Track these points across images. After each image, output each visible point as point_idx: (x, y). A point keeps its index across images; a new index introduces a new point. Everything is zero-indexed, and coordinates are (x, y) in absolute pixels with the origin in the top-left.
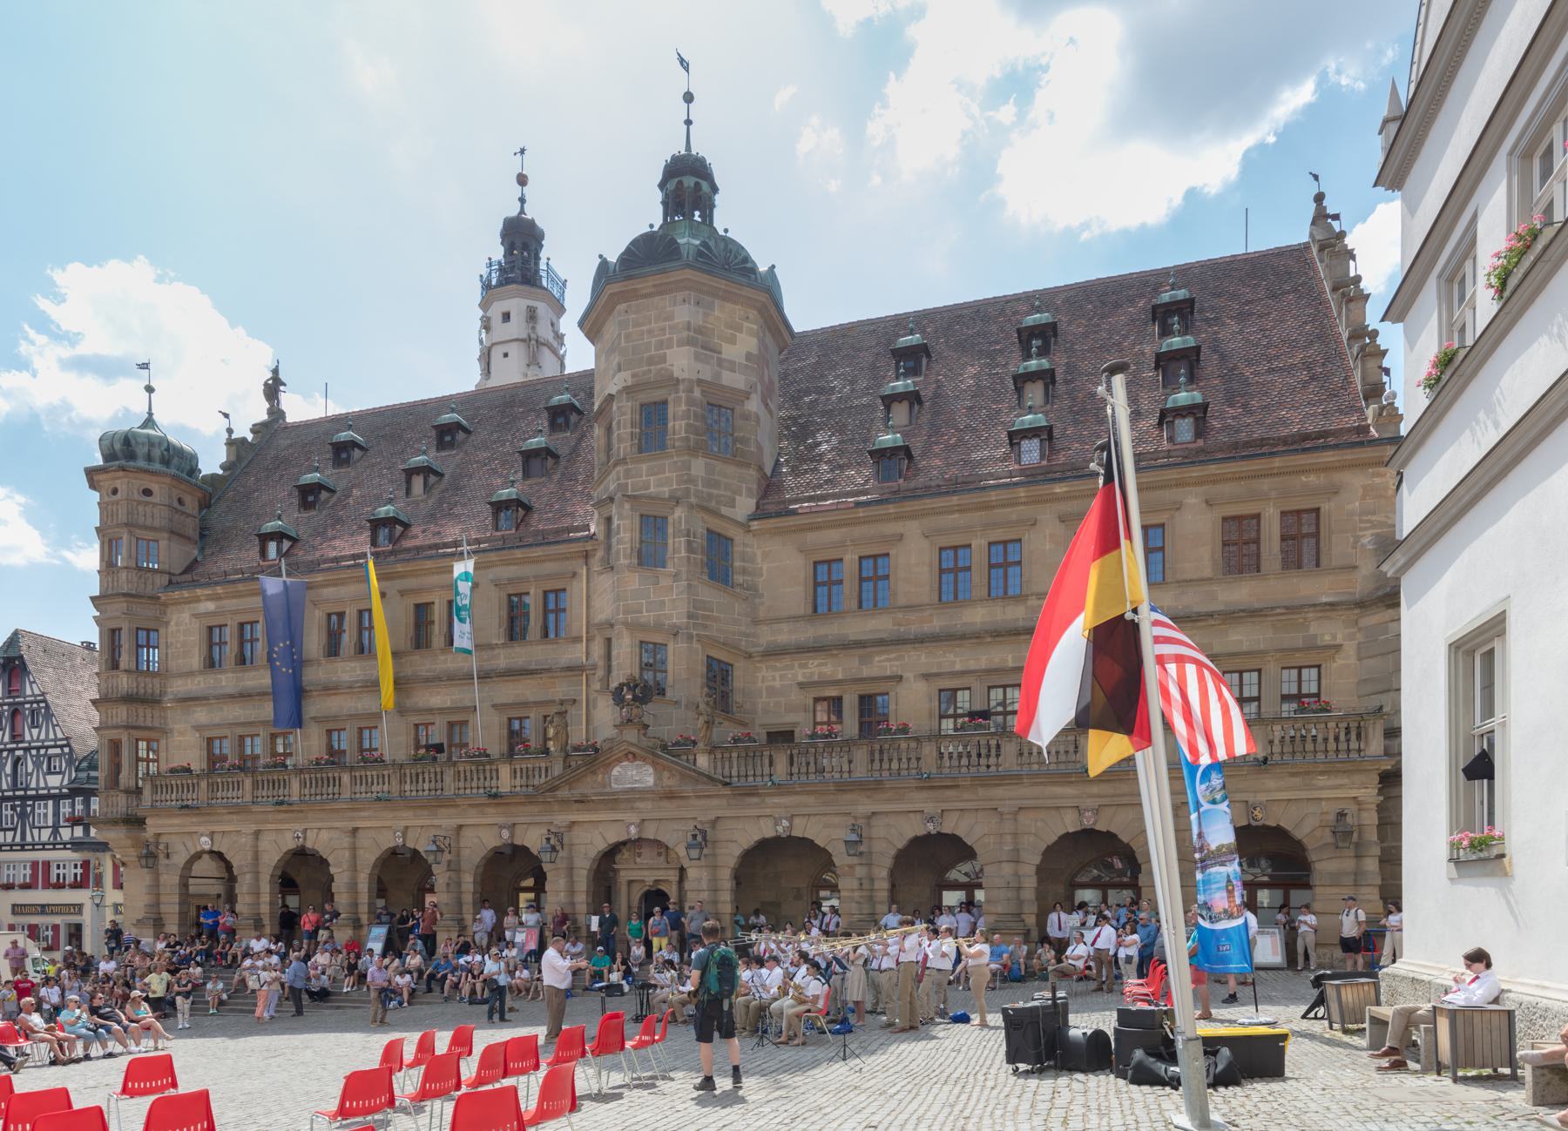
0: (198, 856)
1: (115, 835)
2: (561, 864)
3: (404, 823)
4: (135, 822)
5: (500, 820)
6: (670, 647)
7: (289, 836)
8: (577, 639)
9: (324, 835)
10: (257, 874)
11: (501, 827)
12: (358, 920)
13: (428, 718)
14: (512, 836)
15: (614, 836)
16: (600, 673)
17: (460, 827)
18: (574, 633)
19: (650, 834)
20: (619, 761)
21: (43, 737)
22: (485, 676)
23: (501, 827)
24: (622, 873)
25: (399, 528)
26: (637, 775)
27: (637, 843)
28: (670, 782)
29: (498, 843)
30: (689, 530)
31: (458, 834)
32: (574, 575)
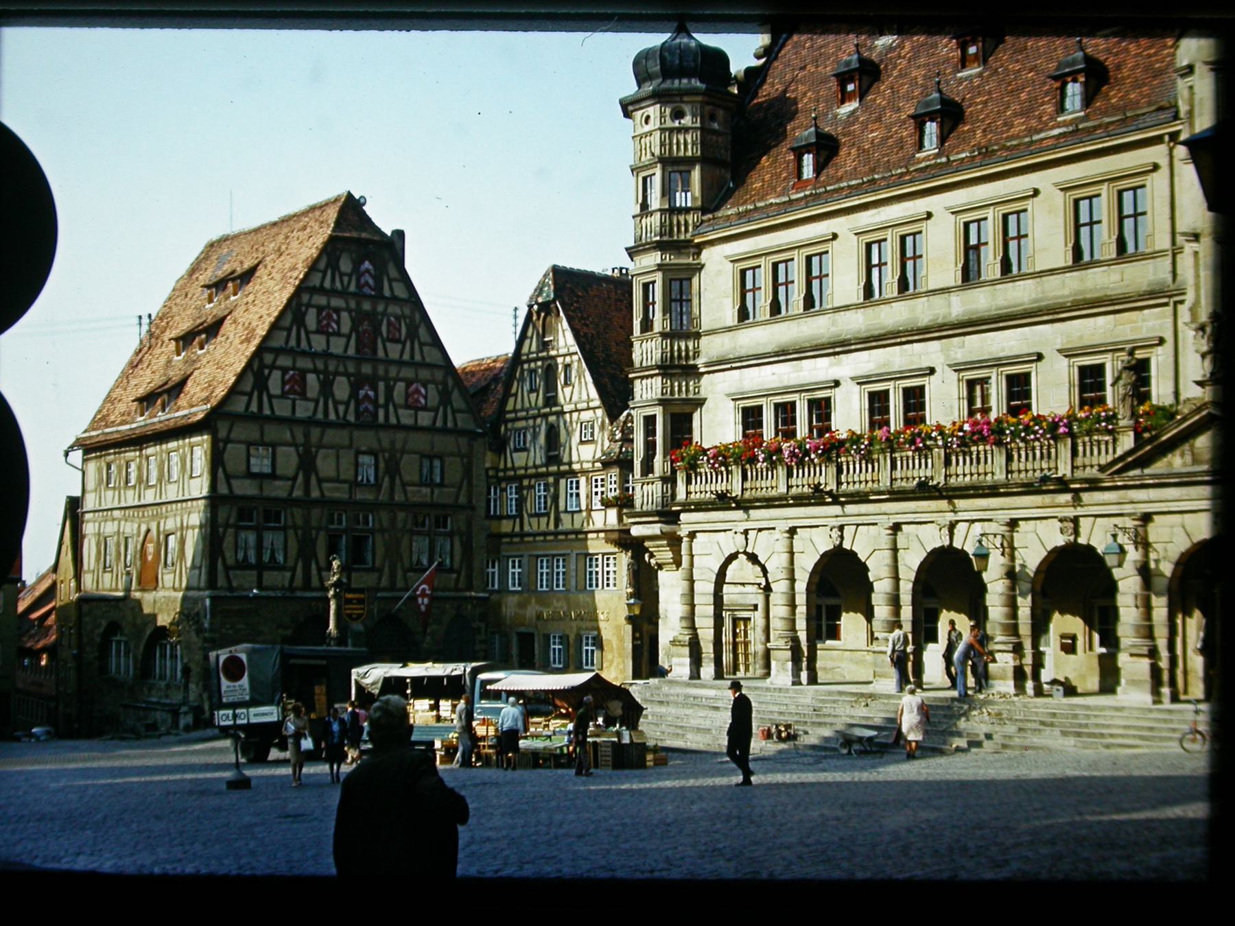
10: (792, 580)
21: (575, 398)
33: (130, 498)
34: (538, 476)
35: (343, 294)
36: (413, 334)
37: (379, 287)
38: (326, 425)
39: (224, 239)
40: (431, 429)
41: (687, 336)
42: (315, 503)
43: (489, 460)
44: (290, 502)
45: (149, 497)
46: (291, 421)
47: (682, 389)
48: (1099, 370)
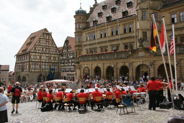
0: (86, 67)
1: (76, 65)
4: (78, 63)
6: (147, 32)
9: (100, 64)
10: (92, 70)
12: (104, 77)
13: (114, 46)
14: (124, 64)
15: (139, 64)
24: (141, 70)
26: (141, 54)
27: (143, 65)
28: (147, 55)
30: (150, 13)
33: (21, 61)
34: (66, 59)
35: (45, 39)
36: (52, 44)
37: (49, 38)
38: (43, 53)
39: (33, 33)
40: (54, 54)
41: (81, 42)
42: (41, 62)
43: (61, 58)
44: (38, 62)
45: (23, 61)
46: (39, 53)
47: (80, 48)
48: (127, 45)
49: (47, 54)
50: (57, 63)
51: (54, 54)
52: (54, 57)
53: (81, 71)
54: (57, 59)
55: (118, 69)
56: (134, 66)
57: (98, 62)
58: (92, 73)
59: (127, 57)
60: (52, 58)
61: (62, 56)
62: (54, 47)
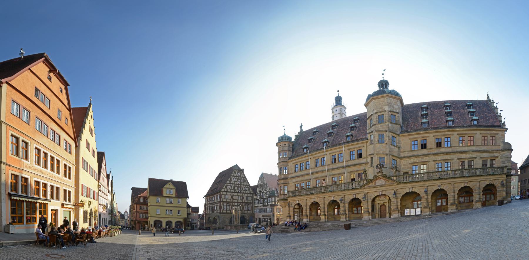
2: (366, 201)
3: (333, 195)
5: (354, 193)
7: (312, 199)
8: (365, 158)
11: (353, 194)
14: (356, 196)
16: (370, 164)
17: (345, 195)
18: (364, 157)
19: (383, 193)
20: (377, 179)
22: (346, 167)
23: (353, 194)
25: (328, 143)
29: (353, 198)
31: (344, 197)
32: (364, 146)
40: (247, 193)
43: (255, 197)
49: (239, 193)
50: (250, 203)
51: (247, 193)
52: (246, 197)
53: (291, 209)
54: (250, 198)
55: (346, 203)
56: (369, 198)
57: (316, 196)
58: (306, 210)
59: (359, 187)
60: (245, 198)
61: (256, 195)
62: (246, 185)
